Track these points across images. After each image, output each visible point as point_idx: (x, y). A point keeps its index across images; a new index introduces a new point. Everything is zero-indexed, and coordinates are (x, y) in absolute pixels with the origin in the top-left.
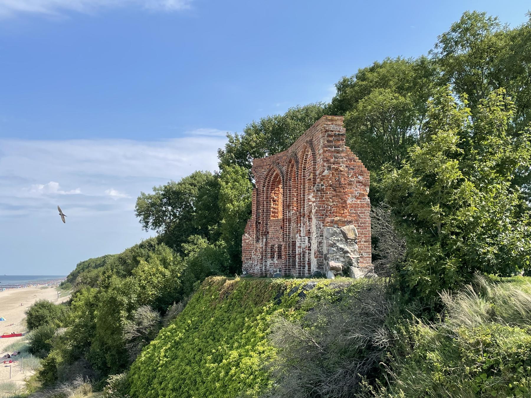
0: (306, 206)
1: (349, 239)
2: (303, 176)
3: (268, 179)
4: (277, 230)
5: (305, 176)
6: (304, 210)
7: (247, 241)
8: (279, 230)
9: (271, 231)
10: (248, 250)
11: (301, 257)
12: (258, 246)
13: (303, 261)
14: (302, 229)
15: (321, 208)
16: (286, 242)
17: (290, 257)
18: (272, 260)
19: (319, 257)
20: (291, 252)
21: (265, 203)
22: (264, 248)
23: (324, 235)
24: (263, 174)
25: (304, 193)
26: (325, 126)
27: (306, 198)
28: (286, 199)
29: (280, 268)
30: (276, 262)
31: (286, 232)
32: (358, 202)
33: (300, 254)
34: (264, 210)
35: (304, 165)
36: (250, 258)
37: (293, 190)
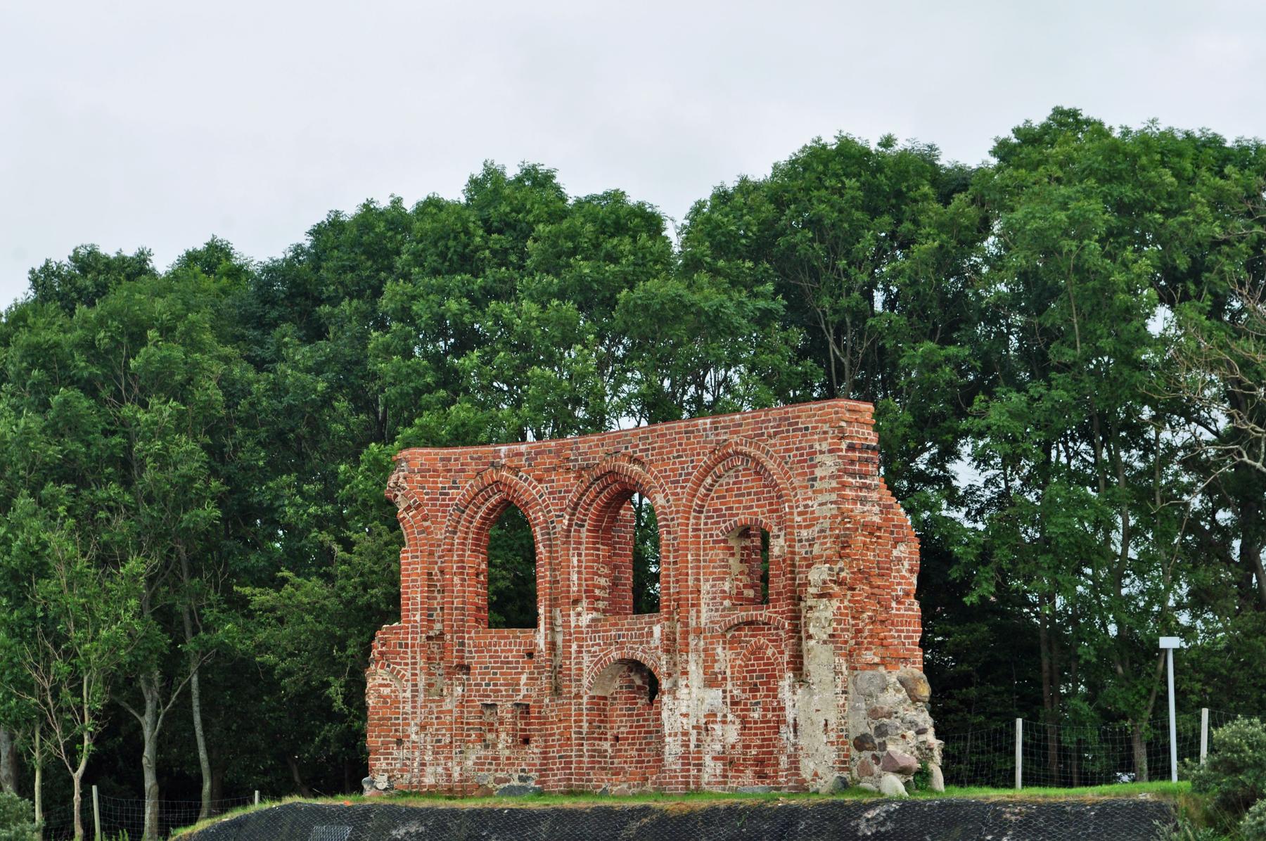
0: (704, 608)
1: (919, 701)
2: (694, 530)
3: (467, 511)
4: (508, 663)
5: (700, 530)
6: (698, 617)
7: (386, 691)
8: (517, 662)
9: (477, 663)
10: (391, 719)
11: (689, 740)
12: (433, 705)
13: (699, 752)
14: (692, 667)
15: (842, 626)
16: (570, 698)
17: (583, 739)
18: (487, 747)
19: (844, 743)
20: (585, 725)
21: (456, 580)
22: (455, 715)
23: (851, 689)
24: (441, 494)
25: (699, 574)
26: (843, 424)
27: (705, 587)
28: (569, 579)
29: (523, 770)
30: (507, 752)
31: (570, 669)
32: (902, 612)
33: (685, 734)
34: (453, 603)
35: (703, 500)
36: (399, 742)
37: (592, 555)
